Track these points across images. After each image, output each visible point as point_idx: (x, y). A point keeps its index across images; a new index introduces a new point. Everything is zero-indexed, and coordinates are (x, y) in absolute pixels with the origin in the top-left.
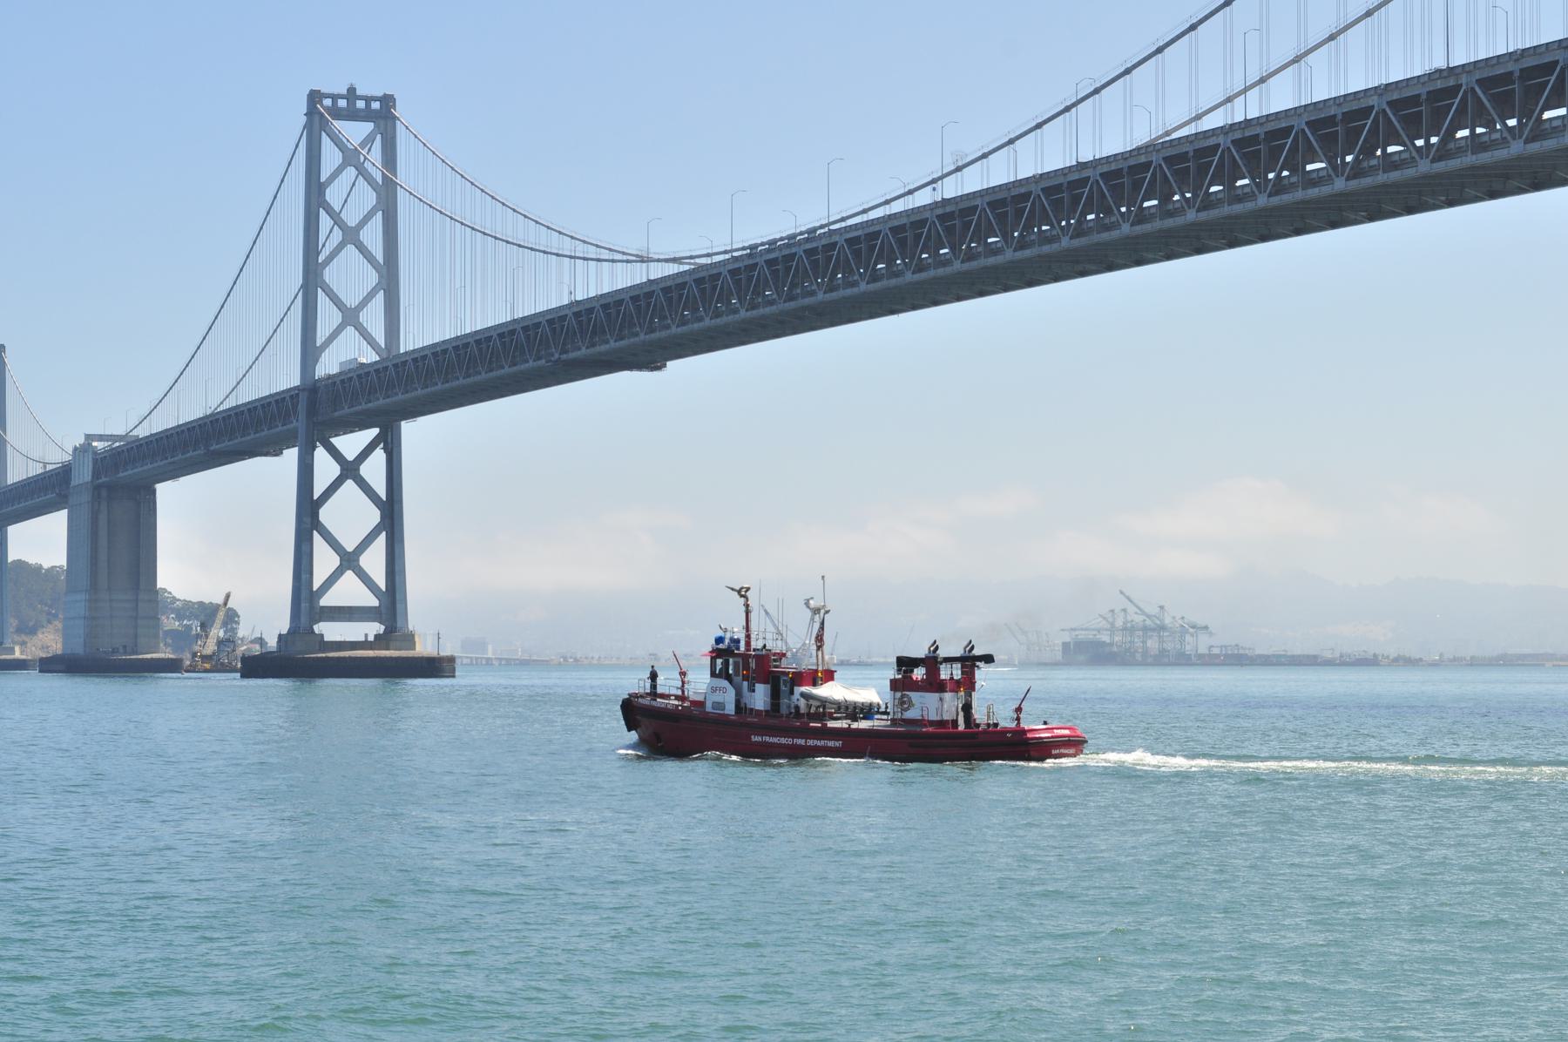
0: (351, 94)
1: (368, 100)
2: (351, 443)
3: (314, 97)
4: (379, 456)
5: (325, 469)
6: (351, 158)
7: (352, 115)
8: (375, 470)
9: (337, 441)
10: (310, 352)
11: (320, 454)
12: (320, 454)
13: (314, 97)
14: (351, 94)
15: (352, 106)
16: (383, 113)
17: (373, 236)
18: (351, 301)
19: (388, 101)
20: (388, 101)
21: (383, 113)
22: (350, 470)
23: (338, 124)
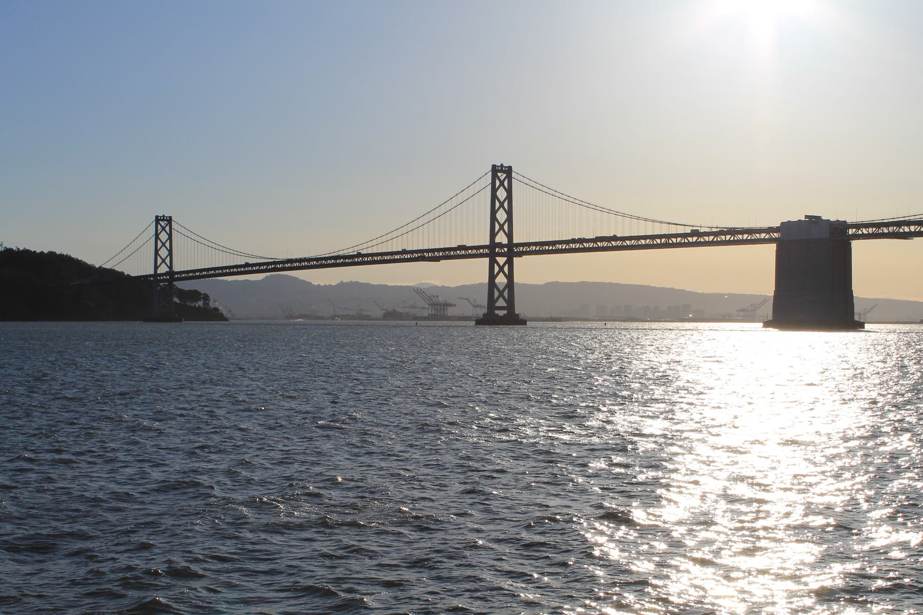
0: (164, 216)
1: (167, 217)
3: (157, 217)
6: (164, 229)
7: (163, 220)
10: (156, 267)
13: (157, 217)
14: (164, 216)
15: (163, 218)
16: (169, 220)
17: (168, 245)
18: (164, 258)
19: (170, 217)
20: (170, 217)
21: (169, 220)
23: (162, 223)
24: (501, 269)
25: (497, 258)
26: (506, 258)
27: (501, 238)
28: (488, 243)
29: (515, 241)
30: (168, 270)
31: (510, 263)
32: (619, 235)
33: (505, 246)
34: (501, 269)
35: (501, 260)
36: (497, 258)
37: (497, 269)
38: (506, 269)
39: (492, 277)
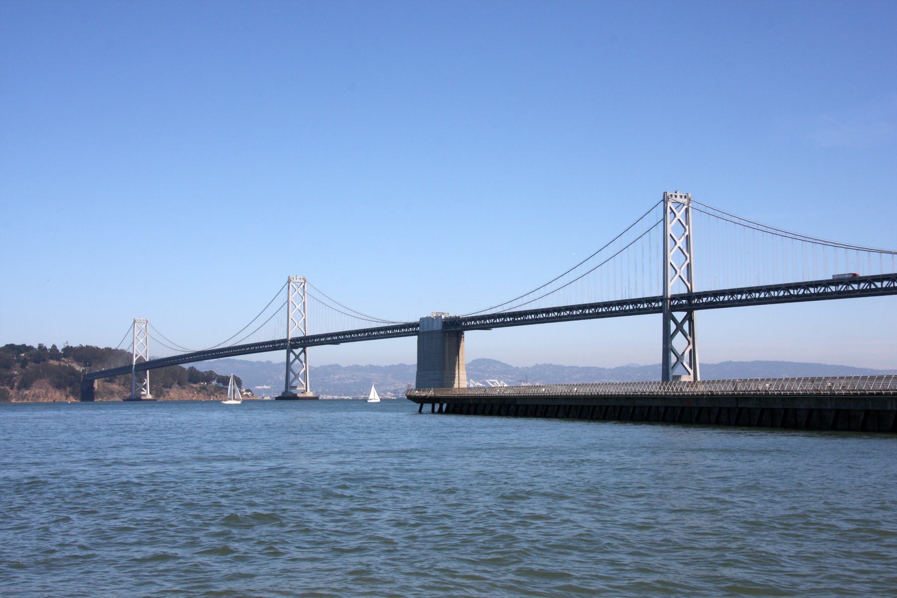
2: (297, 351)
4: (303, 354)
5: (292, 357)
8: (302, 357)
9: (294, 350)
11: (291, 354)
12: (291, 354)
22: (297, 357)
24: (679, 327)
25: (674, 313)
26: (685, 313)
27: (676, 287)
28: (660, 294)
29: (697, 287)
30: (303, 336)
31: (690, 318)
32: (861, 275)
33: (680, 297)
34: (679, 327)
35: (680, 316)
36: (674, 313)
37: (673, 327)
38: (686, 327)
39: (667, 337)
